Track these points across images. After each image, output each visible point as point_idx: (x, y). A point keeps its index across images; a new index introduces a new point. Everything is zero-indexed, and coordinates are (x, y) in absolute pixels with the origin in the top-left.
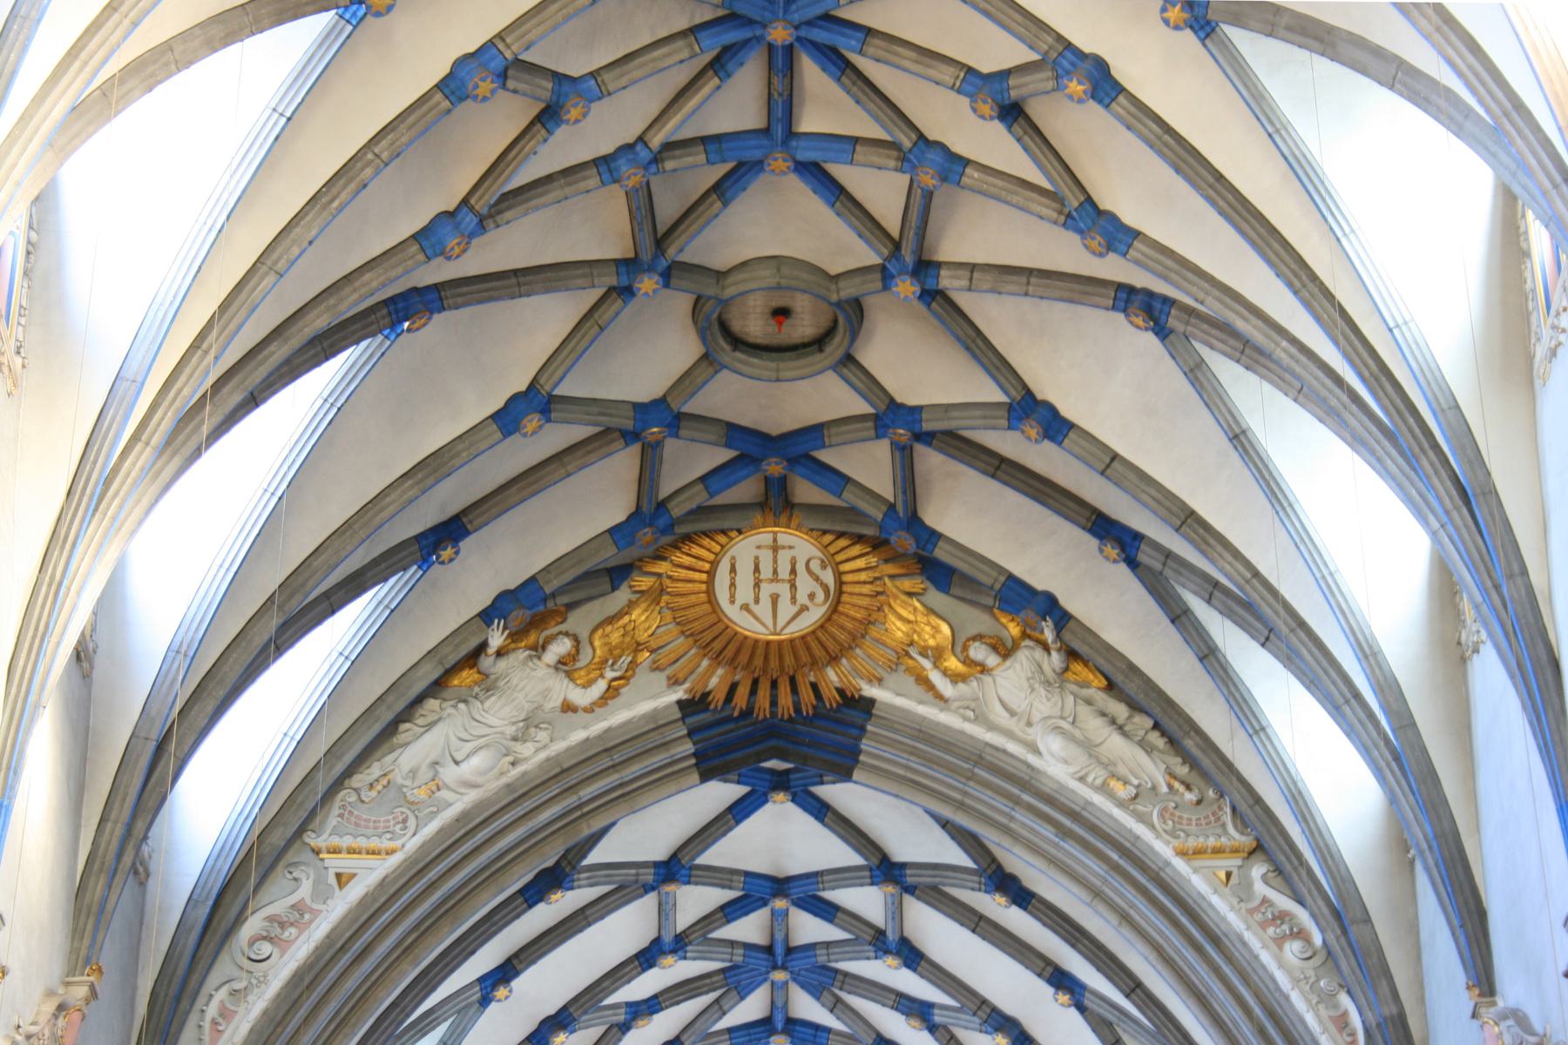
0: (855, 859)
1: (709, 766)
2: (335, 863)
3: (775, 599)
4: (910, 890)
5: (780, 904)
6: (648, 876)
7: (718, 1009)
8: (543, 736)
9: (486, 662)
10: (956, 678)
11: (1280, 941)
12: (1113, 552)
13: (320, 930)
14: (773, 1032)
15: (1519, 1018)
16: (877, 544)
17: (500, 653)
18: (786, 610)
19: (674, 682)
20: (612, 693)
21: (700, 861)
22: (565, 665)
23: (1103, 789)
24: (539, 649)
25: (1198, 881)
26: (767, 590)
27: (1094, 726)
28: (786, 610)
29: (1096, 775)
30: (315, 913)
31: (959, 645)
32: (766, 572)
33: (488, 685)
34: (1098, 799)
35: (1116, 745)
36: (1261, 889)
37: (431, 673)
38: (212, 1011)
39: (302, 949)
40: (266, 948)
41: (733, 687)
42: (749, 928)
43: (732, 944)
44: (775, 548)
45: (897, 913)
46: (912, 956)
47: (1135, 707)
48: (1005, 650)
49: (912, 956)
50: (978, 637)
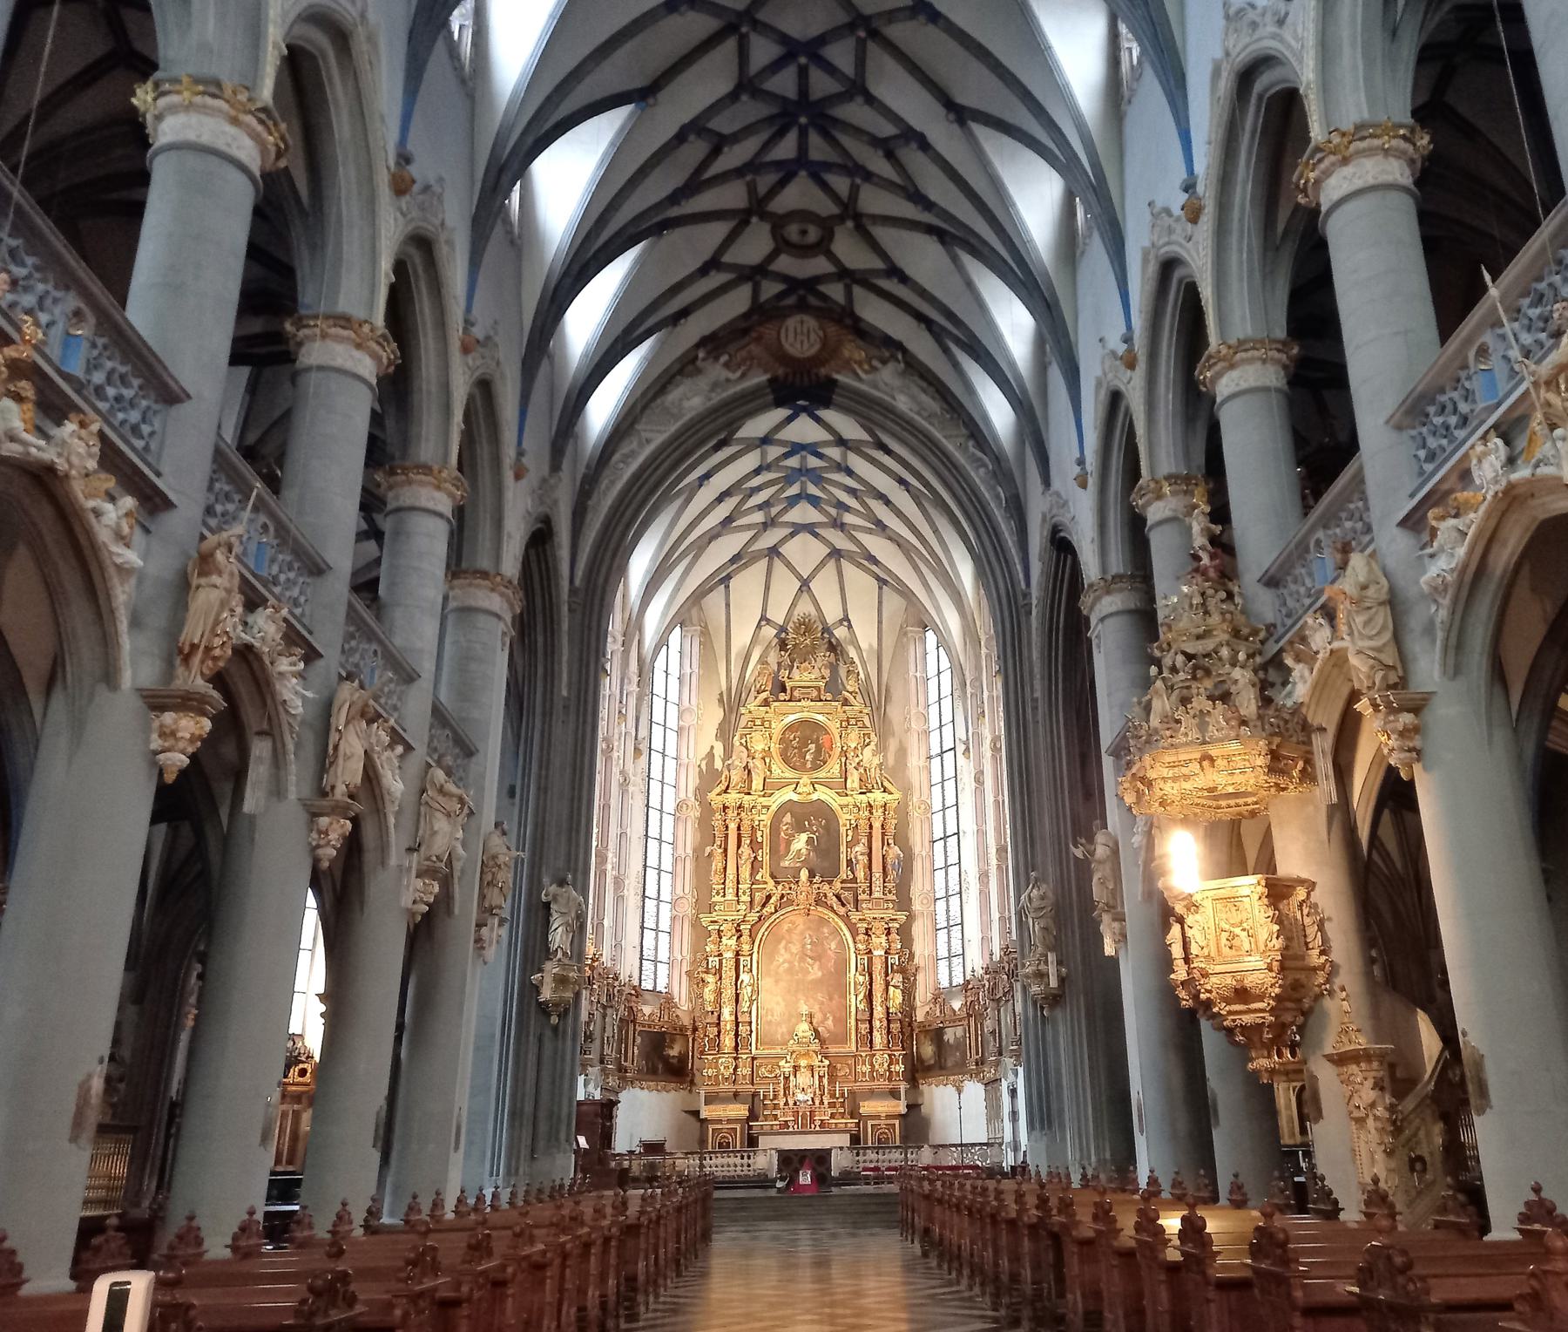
0: (831, 438)
1: (779, 403)
2: (648, 435)
3: (802, 342)
4: (850, 449)
5: (804, 453)
6: (758, 443)
7: (782, 490)
8: (719, 390)
9: (699, 363)
10: (866, 372)
11: (977, 468)
12: (923, 326)
13: (641, 459)
15: (1058, 494)
16: (839, 321)
17: (704, 360)
18: (806, 345)
19: (766, 372)
20: (743, 375)
22: (727, 365)
23: (919, 413)
24: (717, 359)
25: (950, 447)
26: (799, 337)
27: (915, 390)
28: (806, 345)
29: (916, 408)
30: (639, 454)
31: (869, 361)
33: (699, 371)
34: (917, 417)
35: (924, 398)
36: (972, 449)
37: (677, 367)
38: (603, 486)
39: (634, 466)
40: (621, 465)
42: (793, 462)
44: (802, 322)
45: (844, 457)
46: (850, 472)
47: (930, 384)
48: (884, 362)
49: (850, 472)
50: (874, 357)
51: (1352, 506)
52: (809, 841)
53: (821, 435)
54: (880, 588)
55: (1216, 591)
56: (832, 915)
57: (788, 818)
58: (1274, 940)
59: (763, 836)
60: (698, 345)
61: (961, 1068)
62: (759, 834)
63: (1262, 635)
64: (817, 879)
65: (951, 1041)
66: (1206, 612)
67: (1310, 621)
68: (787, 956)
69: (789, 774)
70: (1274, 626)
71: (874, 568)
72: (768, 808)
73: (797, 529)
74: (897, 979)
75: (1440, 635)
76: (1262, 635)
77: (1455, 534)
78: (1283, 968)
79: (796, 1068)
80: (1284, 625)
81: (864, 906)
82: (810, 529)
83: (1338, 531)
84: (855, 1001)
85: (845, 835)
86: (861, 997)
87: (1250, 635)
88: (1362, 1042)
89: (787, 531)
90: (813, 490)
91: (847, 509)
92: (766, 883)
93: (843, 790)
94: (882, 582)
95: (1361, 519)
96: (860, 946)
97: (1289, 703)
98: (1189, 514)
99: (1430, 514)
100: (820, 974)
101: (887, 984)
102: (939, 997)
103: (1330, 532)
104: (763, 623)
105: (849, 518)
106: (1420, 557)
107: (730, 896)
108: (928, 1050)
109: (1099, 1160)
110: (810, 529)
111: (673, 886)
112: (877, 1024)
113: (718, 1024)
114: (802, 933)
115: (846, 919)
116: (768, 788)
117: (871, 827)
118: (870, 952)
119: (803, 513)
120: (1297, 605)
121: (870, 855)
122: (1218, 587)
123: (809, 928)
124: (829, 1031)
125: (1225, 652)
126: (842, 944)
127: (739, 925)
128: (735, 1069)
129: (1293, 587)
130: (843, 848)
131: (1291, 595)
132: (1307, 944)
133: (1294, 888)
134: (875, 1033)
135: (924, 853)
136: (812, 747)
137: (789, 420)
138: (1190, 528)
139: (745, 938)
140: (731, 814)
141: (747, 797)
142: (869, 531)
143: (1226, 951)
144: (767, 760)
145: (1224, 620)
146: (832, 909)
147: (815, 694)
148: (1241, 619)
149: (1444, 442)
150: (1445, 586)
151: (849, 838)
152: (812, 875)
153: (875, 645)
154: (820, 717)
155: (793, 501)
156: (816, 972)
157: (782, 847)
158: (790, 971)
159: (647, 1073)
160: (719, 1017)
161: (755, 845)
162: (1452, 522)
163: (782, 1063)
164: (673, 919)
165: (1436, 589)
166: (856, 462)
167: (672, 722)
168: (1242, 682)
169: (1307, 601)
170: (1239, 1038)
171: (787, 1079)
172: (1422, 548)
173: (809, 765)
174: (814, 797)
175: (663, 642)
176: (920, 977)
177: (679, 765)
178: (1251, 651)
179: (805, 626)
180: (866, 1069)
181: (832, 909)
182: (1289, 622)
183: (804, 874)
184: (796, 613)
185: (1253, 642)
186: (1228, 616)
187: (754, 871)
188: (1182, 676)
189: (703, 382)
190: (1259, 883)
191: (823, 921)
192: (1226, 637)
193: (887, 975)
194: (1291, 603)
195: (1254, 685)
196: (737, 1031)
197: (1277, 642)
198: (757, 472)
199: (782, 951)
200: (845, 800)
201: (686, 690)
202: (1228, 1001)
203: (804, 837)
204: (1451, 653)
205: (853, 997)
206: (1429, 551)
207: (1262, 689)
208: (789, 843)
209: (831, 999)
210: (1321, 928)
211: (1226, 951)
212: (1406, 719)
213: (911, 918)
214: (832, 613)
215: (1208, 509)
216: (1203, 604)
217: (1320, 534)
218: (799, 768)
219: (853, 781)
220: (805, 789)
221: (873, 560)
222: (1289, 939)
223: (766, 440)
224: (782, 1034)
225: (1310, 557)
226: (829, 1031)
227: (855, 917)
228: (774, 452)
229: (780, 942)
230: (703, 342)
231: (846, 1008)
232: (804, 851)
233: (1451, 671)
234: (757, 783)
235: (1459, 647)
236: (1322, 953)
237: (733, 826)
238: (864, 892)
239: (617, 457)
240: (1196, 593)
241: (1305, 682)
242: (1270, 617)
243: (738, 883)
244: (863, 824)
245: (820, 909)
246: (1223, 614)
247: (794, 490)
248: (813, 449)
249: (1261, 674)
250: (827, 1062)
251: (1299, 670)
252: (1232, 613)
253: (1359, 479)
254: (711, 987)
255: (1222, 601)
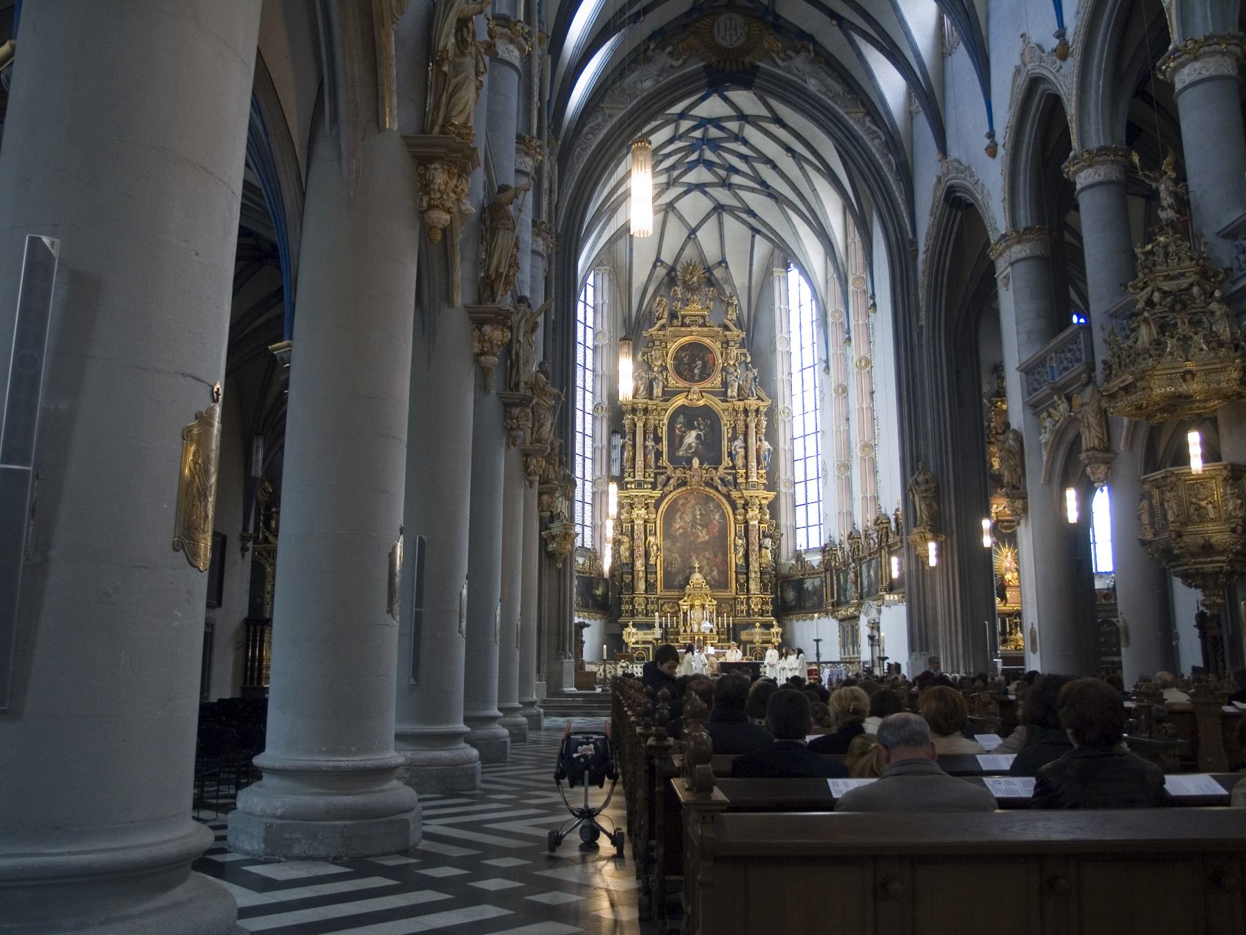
0: (733, 113)
4: (748, 123)
6: (676, 117)
7: (686, 156)
14: (699, 163)
19: (702, 60)
21: (690, 113)
31: (784, 51)
32: (728, 27)
41: (719, 61)
42: (698, 134)
43: (693, 137)
45: (741, 128)
46: (745, 142)
49: (745, 142)
52: (698, 437)
53: (726, 110)
54: (753, 237)
56: (716, 494)
57: (681, 419)
59: (664, 432)
60: (650, 38)
61: (819, 608)
62: (659, 431)
64: (706, 466)
65: (810, 588)
68: (681, 524)
69: (682, 384)
71: (751, 220)
72: (666, 410)
73: (691, 188)
74: (768, 542)
79: (692, 606)
81: (742, 487)
82: (701, 187)
84: (735, 559)
85: (726, 433)
86: (740, 554)
89: (681, 190)
90: (709, 155)
91: (737, 171)
92: (666, 468)
93: (724, 396)
94: (755, 231)
96: (739, 517)
100: (707, 537)
101: (760, 547)
102: (798, 556)
104: (659, 264)
105: (736, 179)
107: (639, 476)
108: (791, 595)
110: (701, 187)
111: (593, 469)
112: (753, 575)
113: (632, 573)
114: (693, 506)
115: (728, 497)
116: (668, 395)
117: (747, 427)
118: (746, 522)
119: (699, 175)
121: (746, 449)
123: (698, 503)
124: (714, 580)
126: (723, 516)
127: (646, 500)
128: (646, 606)
130: (725, 442)
134: (751, 582)
135: (787, 448)
136: (699, 363)
137: (702, 99)
139: (652, 509)
140: (640, 414)
141: (650, 402)
142: (753, 190)
144: (665, 374)
146: (717, 489)
147: (701, 321)
151: (730, 435)
152: (701, 463)
153: (747, 284)
154: (707, 341)
155: (692, 166)
156: (703, 536)
157: (677, 441)
158: (684, 534)
159: (581, 607)
160: (632, 568)
161: (658, 440)
163: (681, 602)
164: (594, 494)
166: (751, 133)
167: (590, 343)
171: (685, 614)
173: (697, 378)
174: (701, 403)
175: (585, 284)
176: (784, 539)
177: (595, 377)
179: (690, 268)
180: (744, 607)
181: (717, 489)
183: (696, 462)
184: (683, 256)
187: (657, 460)
189: (652, 69)
191: (709, 499)
193: (759, 539)
196: (646, 577)
198: (671, 141)
199: (679, 520)
200: (725, 405)
201: (599, 316)
203: (694, 433)
205: (733, 556)
208: (682, 438)
209: (716, 556)
213: (777, 498)
214: (712, 254)
218: (691, 379)
219: (732, 392)
220: (695, 397)
221: (751, 213)
223: (683, 115)
224: (679, 581)
226: (714, 580)
227: (734, 494)
228: (685, 125)
229: (676, 514)
230: (652, 37)
231: (725, 562)
232: (694, 444)
234: (657, 391)
237: (640, 425)
238: (742, 477)
239: (586, 129)
243: (645, 468)
244: (741, 424)
245: (707, 489)
247: (694, 157)
248: (716, 122)
250: (715, 602)
254: (627, 545)
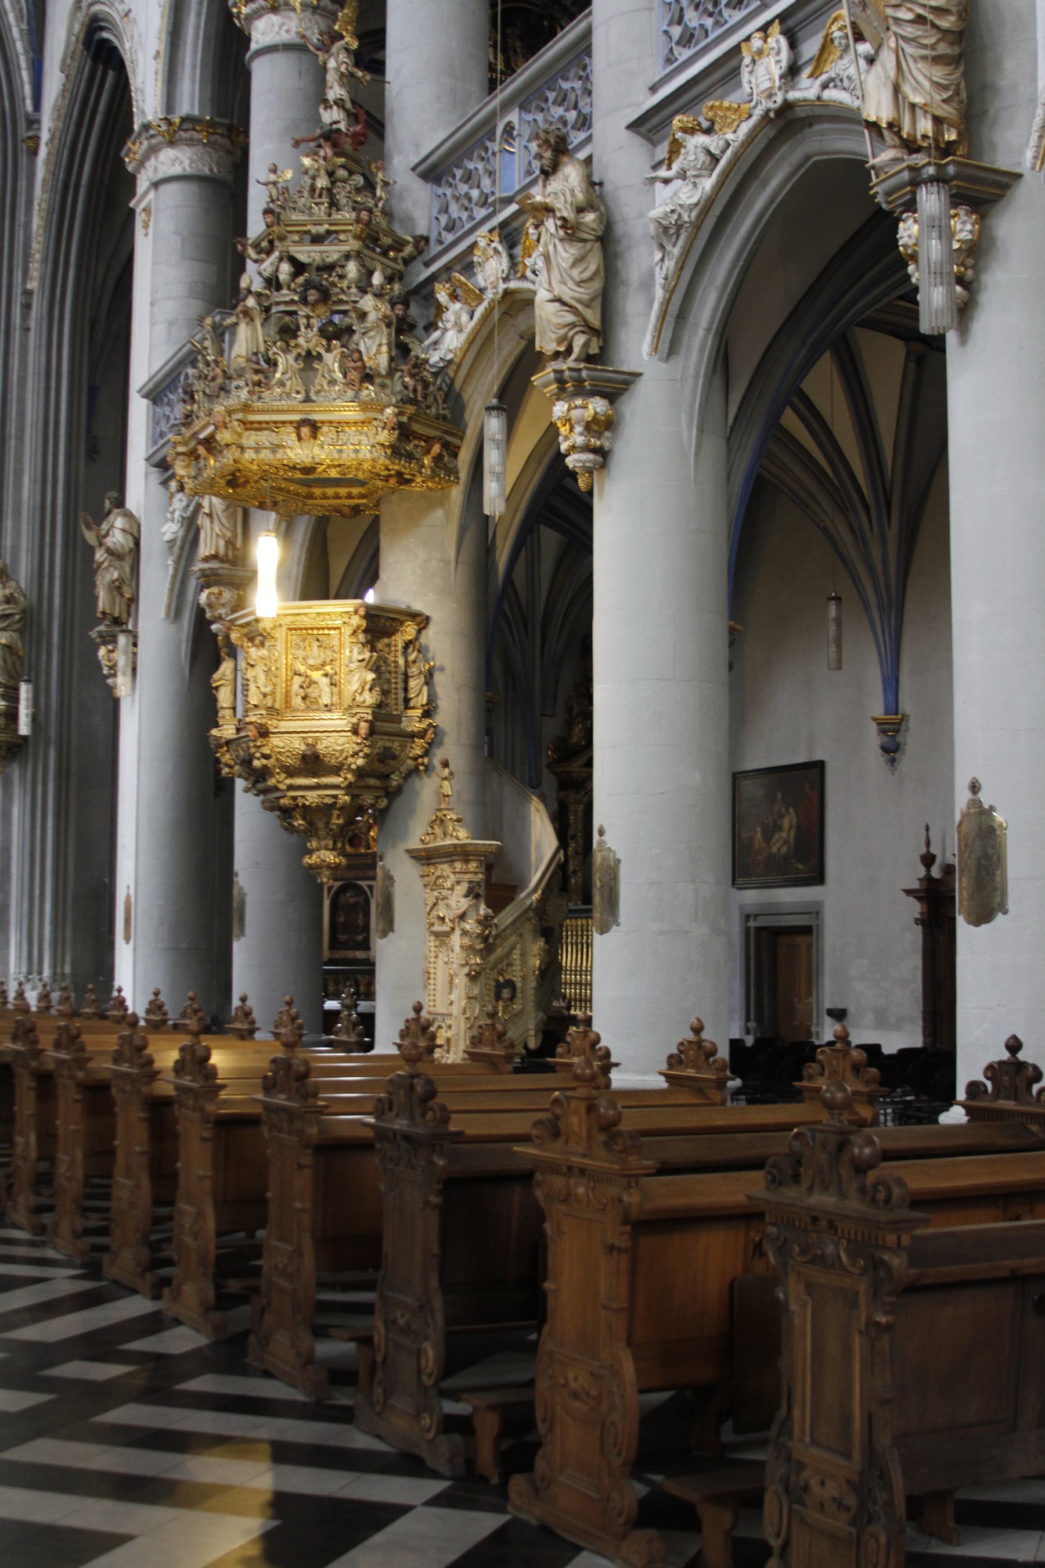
51: (566, 86)
55: (351, 173)
58: (366, 694)
63: (408, 250)
66: (334, 204)
67: (482, 243)
70: (426, 240)
75: (659, 294)
76: (408, 250)
77: (703, 157)
78: (372, 732)
80: (441, 242)
83: (540, 117)
87: (391, 248)
88: (462, 835)
95: (575, 107)
97: (434, 358)
98: (325, 48)
99: (676, 122)
103: (529, 117)
106: (653, 180)
109: (55, 974)
120: (465, 215)
122: (354, 167)
125: (352, 269)
129: (463, 188)
131: (457, 199)
132: (407, 700)
133: (402, 623)
138: (324, 69)
143: (297, 701)
145: (358, 220)
148: (379, 218)
149: (709, 22)
150: (679, 227)
162: (701, 139)
165: (666, 229)
168: (372, 317)
169: (480, 213)
170: (299, 822)
172: (655, 167)
178: (389, 271)
182: (449, 238)
185: (395, 260)
186: (364, 215)
188: (285, 295)
190: (356, 612)
192: (353, 245)
194: (454, 209)
195: (388, 325)
197: (427, 265)
202: (290, 772)
204: (670, 320)
206: (663, 173)
207: (399, 332)
210: (429, 678)
211: (297, 701)
212: (597, 406)
215: (355, 45)
216: (329, 190)
217: (513, 116)
222: (385, 693)
225: (494, 147)
233: (664, 347)
235: (682, 316)
236: (427, 714)
240: (323, 172)
241: (460, 331)
242: (421, 230)
246: (356, 208)
249: (399, 310)
251: (455, 311)
252: (370, 211)
253: (583, 47)
255: (358, 190)
